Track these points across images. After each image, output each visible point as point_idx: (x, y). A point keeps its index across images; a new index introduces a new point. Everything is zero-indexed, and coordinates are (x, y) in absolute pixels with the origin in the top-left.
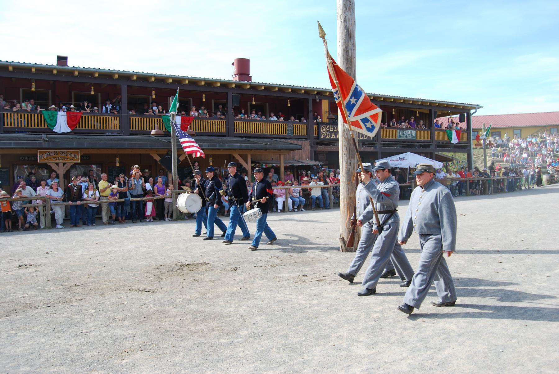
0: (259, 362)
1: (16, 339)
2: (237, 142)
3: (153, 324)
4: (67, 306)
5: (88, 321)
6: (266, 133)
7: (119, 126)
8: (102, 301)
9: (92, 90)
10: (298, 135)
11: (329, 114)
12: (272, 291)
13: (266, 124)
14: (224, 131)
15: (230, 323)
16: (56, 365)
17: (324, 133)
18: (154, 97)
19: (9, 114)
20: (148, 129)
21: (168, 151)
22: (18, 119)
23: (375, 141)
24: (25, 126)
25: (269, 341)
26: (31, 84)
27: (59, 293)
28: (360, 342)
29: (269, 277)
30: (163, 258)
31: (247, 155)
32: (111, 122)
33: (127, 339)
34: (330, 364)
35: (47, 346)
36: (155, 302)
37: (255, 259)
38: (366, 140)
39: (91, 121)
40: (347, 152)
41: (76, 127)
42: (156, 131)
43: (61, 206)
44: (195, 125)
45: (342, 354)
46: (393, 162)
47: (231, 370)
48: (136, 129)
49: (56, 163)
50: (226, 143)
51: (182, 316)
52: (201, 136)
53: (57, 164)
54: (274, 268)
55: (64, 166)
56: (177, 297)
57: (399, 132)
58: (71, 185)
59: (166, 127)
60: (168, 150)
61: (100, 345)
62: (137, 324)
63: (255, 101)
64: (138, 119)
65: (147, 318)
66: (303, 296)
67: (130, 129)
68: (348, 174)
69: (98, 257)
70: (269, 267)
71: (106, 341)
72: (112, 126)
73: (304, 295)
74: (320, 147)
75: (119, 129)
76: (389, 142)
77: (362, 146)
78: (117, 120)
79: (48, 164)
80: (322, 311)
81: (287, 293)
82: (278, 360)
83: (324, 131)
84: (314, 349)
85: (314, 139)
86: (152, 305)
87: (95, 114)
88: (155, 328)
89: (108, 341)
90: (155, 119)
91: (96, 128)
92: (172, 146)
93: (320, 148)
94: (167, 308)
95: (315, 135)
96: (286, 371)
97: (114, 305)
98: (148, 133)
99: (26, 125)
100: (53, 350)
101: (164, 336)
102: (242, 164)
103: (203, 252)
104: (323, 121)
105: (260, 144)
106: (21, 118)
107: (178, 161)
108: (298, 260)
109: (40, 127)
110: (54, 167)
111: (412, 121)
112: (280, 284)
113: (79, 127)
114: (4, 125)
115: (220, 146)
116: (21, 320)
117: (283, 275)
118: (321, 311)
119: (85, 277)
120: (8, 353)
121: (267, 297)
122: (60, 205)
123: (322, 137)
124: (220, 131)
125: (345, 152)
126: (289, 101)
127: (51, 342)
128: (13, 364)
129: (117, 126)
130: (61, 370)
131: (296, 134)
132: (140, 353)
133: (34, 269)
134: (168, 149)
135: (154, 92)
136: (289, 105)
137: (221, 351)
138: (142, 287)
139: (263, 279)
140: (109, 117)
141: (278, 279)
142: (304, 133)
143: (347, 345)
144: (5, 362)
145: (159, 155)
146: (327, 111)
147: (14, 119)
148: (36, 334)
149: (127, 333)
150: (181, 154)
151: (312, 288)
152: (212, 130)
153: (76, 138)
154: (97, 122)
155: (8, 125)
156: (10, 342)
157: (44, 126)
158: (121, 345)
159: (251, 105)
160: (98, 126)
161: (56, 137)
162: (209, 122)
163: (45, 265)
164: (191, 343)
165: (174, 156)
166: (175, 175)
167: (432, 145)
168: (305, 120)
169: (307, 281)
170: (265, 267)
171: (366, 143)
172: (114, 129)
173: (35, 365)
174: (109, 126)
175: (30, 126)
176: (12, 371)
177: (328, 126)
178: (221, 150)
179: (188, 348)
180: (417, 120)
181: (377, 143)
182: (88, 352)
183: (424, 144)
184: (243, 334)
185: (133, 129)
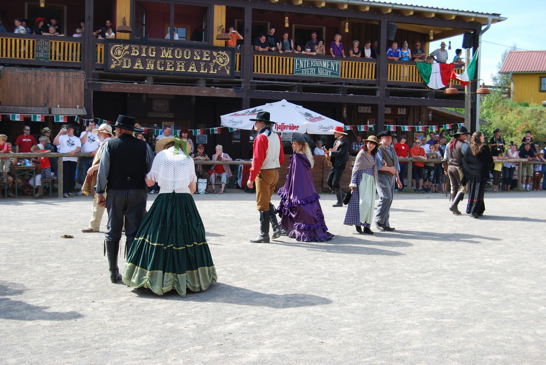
10: (62, 60)
17: (117, 58)
38: (213, 76)
57: (299, 62)
74: (108, 85)
77: (207, 86)
83: (117, 56)
85: (96, 69)
111: (338, 43)
123: (113, 66)
131: (57, 60)
142: (75, 58)
167: (377, 89)
177: (127, 47)
180: (347, 44)
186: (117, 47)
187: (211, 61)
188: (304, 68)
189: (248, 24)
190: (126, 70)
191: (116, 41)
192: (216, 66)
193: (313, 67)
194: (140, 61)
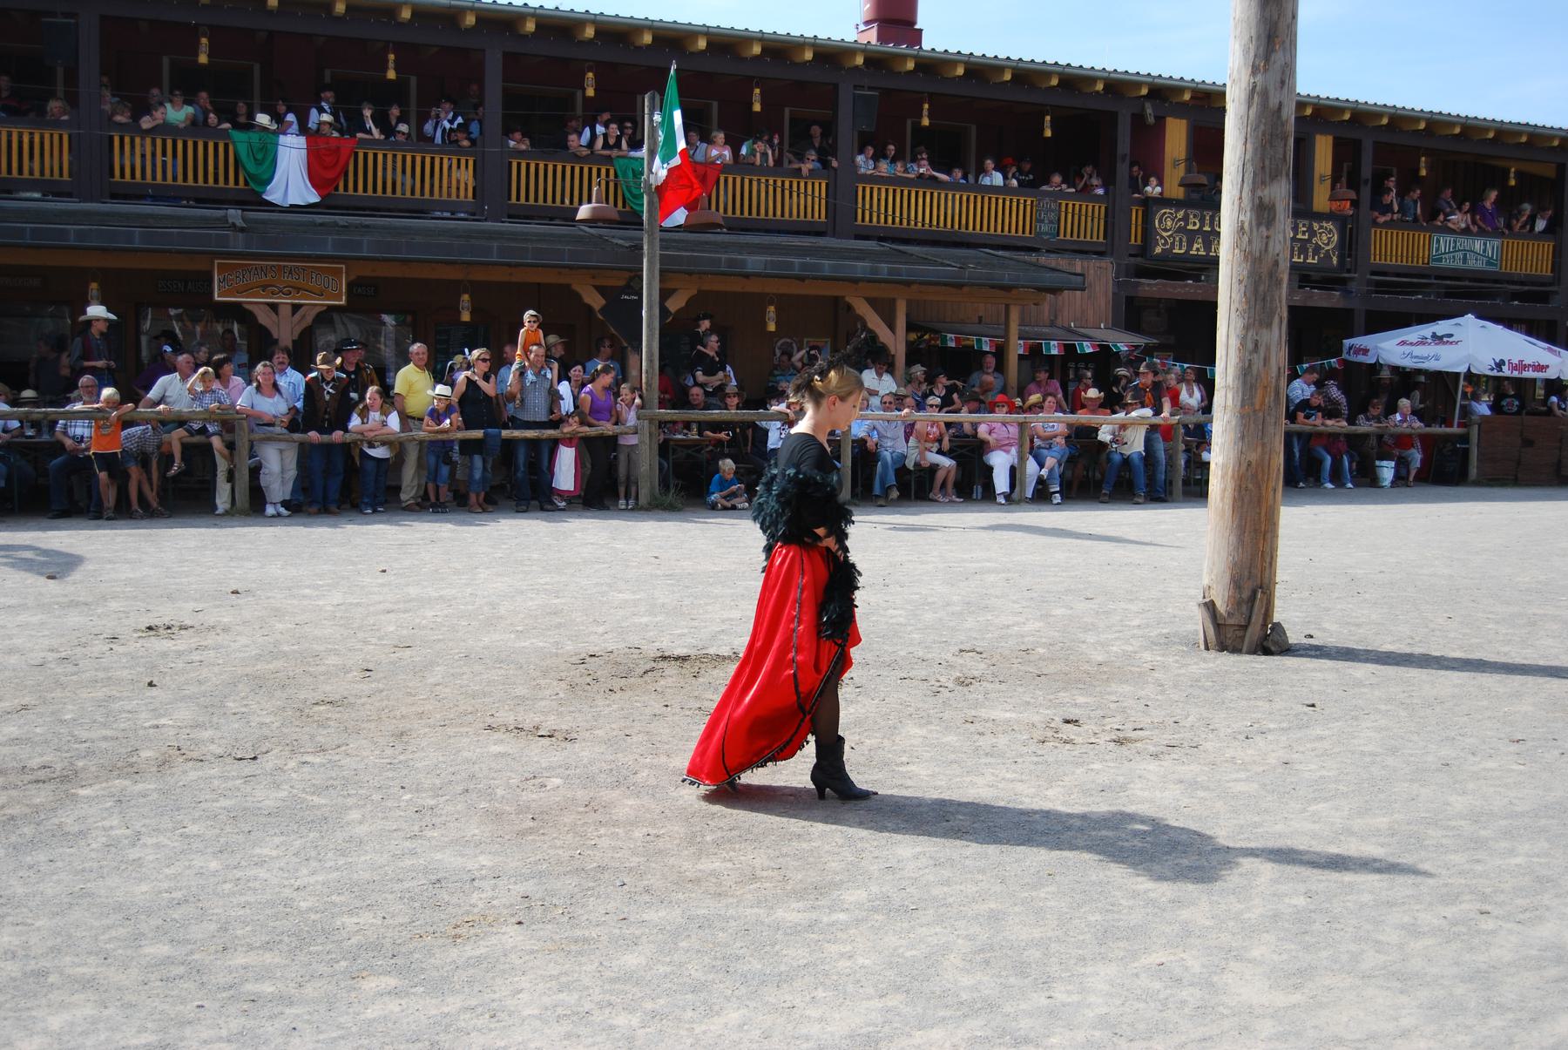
0: (901, 997)
1: (134, 854)
2: (861, 255)
3: (559, 843)
4: (292, 764)
5: (355, 815)
6: (963, 230)
7: (474, 188)
8: (402, 758)
9: (391, 65)
10: (1075, 238)
11: (1188, 170)
12: (955, 766)
13: (965, 198)
14: (819, 215)
15: (811, 860)
16: (251, 948)
17: (1165, 234)
18: (590, 92)
19: (127, 140)
20: (567, 201)
21: (631, 279)
22: (154, 155)
23: (1349, 271)
24: (175, 179)
25: (938, 929)
26: (198, 43)
27: (268, 721)
28: (1250, 961)
29: (946, 716)
30: (601, 630)
31: (894, 300)
32: (450, 176)
33: (476, 884)
34: (1141, 1026)
35: (227, 886)
36: (568, 772)
37: (902, 653)
39: (385, 169)
40: (1248, 302)
41: (336, 189)
42: (594, 208)
43: (283, 446)
44: (722, 192)
45: (1184, 994)
46: (1407, 349)
47: (808, 1012)
48: (527, 199)
49: (268, 304)
50: (823, 257)
51: (653, 824)
52: (742, 230)
53: (274, 307)
54: (965, 689)
55: (293, 314)
56: (642, 760)
57: (1438, 241)
58: (316, 378)
59: (628, 195)
60: (632, 274)
61: (388, 896)
62: (507, 837)
63: (930, 117)
64: (537, 165)
65: (541, 819)
66: (1059, 789)
67: (510, 199)
68: (1244, 383)
69: (391, 616)
70: (951, 685)
71: (406, 885)
72: (449, 187)
73: (1064, 787)
74: (1149, 285)
75: (474, 196)
76: (1398, 275)
77: (1300, 287)
78: (467, 167)
79: (247, 306)
80: (1126, 844)
81: (1008, 776)
82: (964, 996)
83: (1165, 230)
84: (1089, 970)
85: (1131, 255)
86: (558, 781)
87: (396, 146)
88: (565, 855)
89: (415, 883)
90: (590, 169)
91: (399, 194)
92: (645, 260)
93: (1151, 287)
94: (607, 795)
95: (1133, 242)
96: (989, 1033)
97: (438, 772)
98: (569, 216)
99: (180, 177)
100: (243, 899)
101: (591, 884)
102: (878, 331)
103: (732, 620)
104: (1167, 195)
105: (942, 265)
106: (164, 154)
107: (664, 311)
108: (1051, 669)
109: (221, 184)
110: (264, 318)
112: (982, 741)
113: (346, 188)
114: (112, 175)
115: (804, 266)
116: (150, 798)
117: (999, 714)
118: (1120, 843)
119: (350, 675)
120: (107, 897)
121: (939, 783)
122: (280, 440)
123: (1158, 250)
124: (805, 217)
125: (1240, 302)
126: (1048, 118)
127: (239, 874)
128: (122, 931)
129: (466, 189)
130: (268, 961)
131: (1068, 237)
132: (513, 930)
133: (195, 640)
134: (630, 270)
135: (590, 75)
136: (1048, 133)
137: (777, 947)
138: (529, 720)
139: (930, 723)
140: (442, 159)
141: (978, 726)
142: (1094, 232)
143: (1204, 966)
144: (96, 924)
145: (602, 290)
146: (1183, 156)
147: (143, 156)
148: (194, 846)
149: (477, 866)
150: (674, 291)
151: (1092, 766)
152: (779, 213)
153: (336, 224)
154: (404, 172)
155: (122, 175)
156: (115, 864)
157: (237, 182)
158: (454, 900)
159: (917, 128)
160: (406, 186)
161: (271, 220)
162: (771, 182)
163: (226, 630)
164: (679, 911)
165: (649, 295)
166: (650, 361)
168: (1105, 185)
169: (1079, 740)
170: (938, 684)
171: (1315, 275)
172: (458, 196)
173: (188, 942)
174: (441, 187)
175: (190, 182)
176: (120, 951)
177: (1181, 214)
178: (807, 281)
179: (668, 928)
180: (1508, 204)
181: (1352, 279)
182: (350, 913)
183: (1526, 288)
184: (852, 899)
185: (518, 198)
186: (1165, 213)
187: (1309, 241)
188: (1445, 253)
189: (1366, 171)
190: (1178, 257)
191: (1163, 201)
192: (1317, 249)
193: (1459, 250)
194: (1200, 240)
